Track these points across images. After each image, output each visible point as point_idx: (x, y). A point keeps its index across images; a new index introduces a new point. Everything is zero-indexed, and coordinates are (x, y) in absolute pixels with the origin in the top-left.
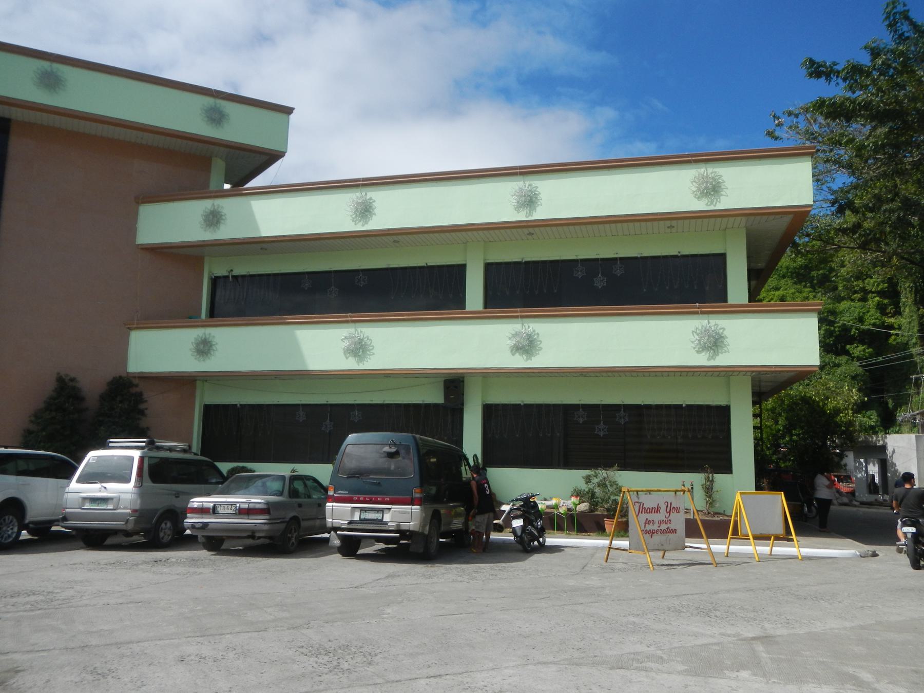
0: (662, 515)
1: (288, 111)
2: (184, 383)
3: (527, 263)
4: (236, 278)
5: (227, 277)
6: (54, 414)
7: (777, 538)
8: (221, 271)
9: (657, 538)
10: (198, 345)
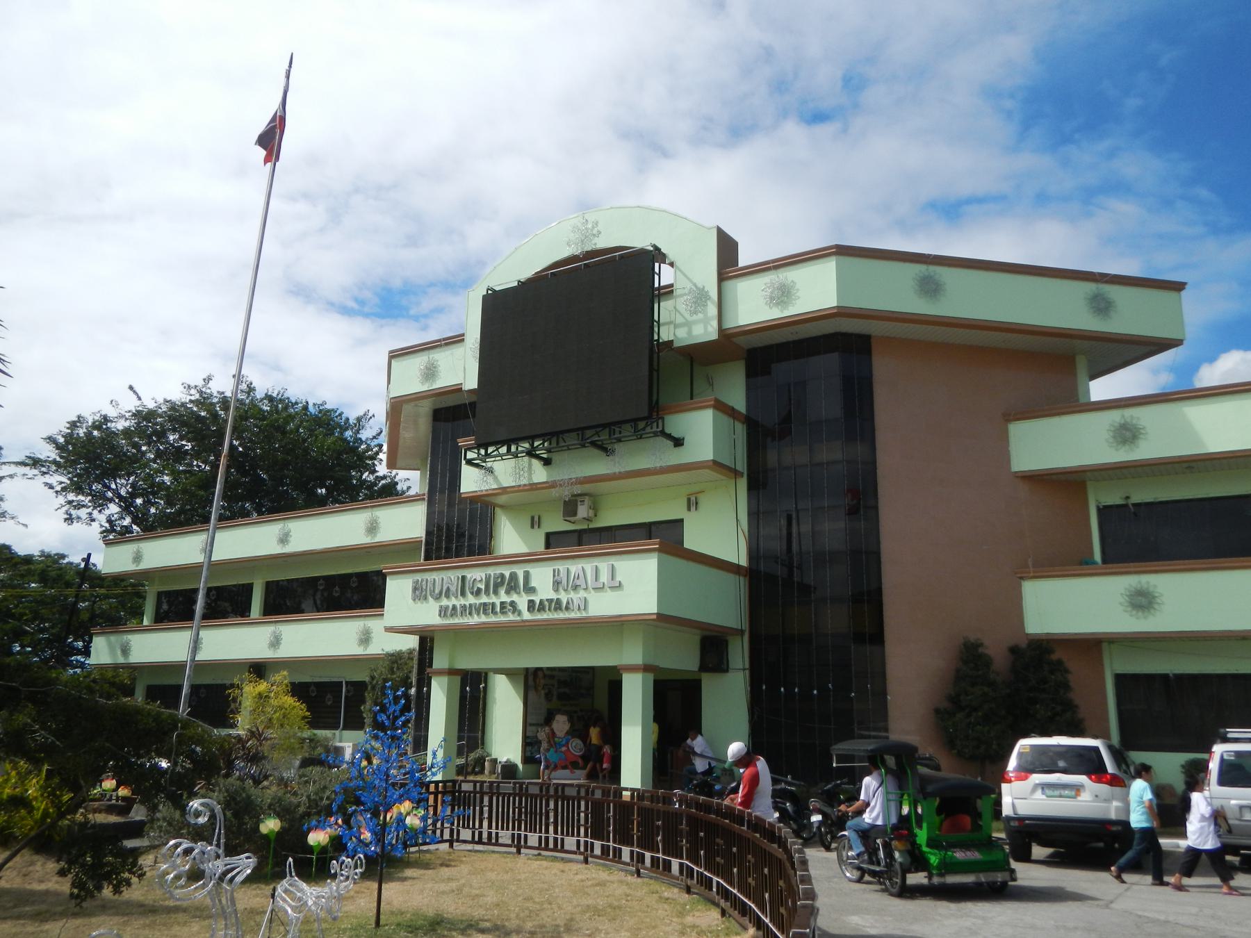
1: (1178, 287)
2: (1091, 646)
4: (1134, 505)
5: (1125, 506)
6: (986, 689)
8: (1114, 499)
10: (1130, 596)
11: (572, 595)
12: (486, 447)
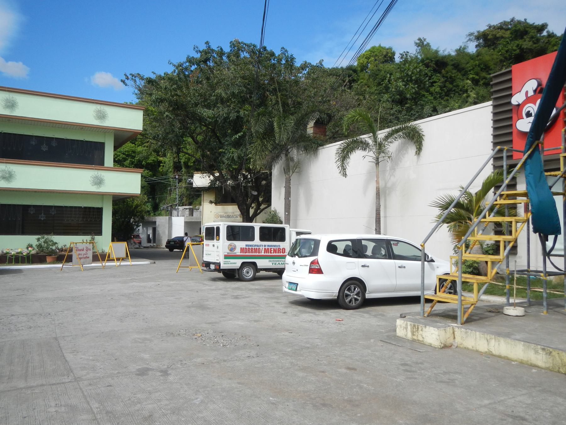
0: (84, 252)
3: (5, 133)
7: (123, 259)
9: (82, 260)
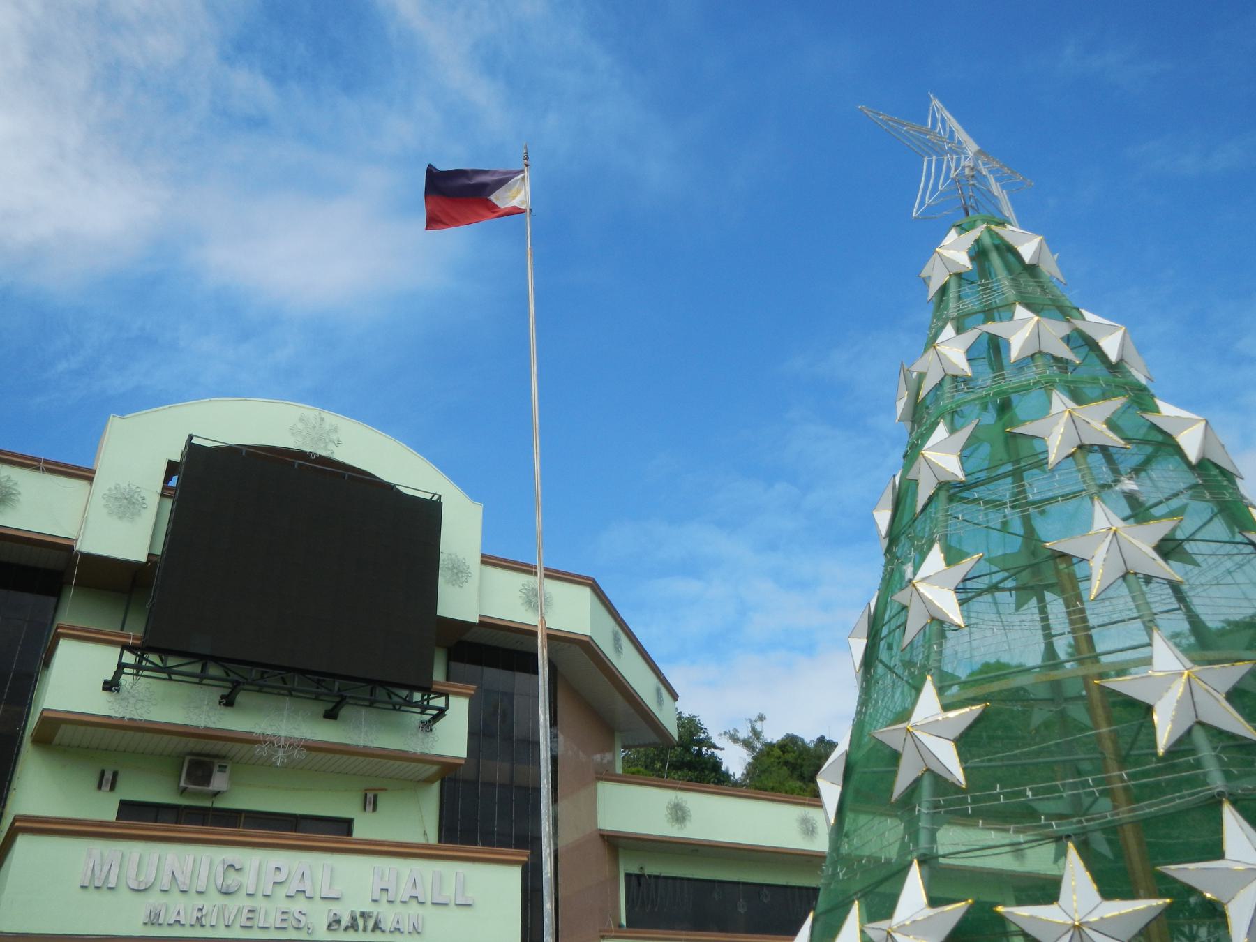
8: (634, 870)
11: (399, 908)
12: (163, 652)
